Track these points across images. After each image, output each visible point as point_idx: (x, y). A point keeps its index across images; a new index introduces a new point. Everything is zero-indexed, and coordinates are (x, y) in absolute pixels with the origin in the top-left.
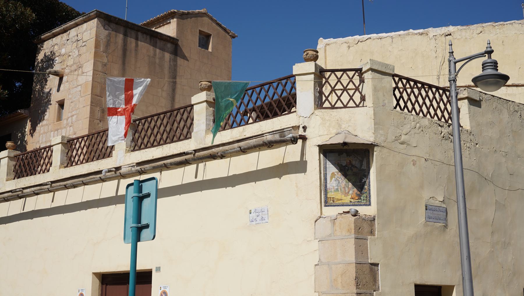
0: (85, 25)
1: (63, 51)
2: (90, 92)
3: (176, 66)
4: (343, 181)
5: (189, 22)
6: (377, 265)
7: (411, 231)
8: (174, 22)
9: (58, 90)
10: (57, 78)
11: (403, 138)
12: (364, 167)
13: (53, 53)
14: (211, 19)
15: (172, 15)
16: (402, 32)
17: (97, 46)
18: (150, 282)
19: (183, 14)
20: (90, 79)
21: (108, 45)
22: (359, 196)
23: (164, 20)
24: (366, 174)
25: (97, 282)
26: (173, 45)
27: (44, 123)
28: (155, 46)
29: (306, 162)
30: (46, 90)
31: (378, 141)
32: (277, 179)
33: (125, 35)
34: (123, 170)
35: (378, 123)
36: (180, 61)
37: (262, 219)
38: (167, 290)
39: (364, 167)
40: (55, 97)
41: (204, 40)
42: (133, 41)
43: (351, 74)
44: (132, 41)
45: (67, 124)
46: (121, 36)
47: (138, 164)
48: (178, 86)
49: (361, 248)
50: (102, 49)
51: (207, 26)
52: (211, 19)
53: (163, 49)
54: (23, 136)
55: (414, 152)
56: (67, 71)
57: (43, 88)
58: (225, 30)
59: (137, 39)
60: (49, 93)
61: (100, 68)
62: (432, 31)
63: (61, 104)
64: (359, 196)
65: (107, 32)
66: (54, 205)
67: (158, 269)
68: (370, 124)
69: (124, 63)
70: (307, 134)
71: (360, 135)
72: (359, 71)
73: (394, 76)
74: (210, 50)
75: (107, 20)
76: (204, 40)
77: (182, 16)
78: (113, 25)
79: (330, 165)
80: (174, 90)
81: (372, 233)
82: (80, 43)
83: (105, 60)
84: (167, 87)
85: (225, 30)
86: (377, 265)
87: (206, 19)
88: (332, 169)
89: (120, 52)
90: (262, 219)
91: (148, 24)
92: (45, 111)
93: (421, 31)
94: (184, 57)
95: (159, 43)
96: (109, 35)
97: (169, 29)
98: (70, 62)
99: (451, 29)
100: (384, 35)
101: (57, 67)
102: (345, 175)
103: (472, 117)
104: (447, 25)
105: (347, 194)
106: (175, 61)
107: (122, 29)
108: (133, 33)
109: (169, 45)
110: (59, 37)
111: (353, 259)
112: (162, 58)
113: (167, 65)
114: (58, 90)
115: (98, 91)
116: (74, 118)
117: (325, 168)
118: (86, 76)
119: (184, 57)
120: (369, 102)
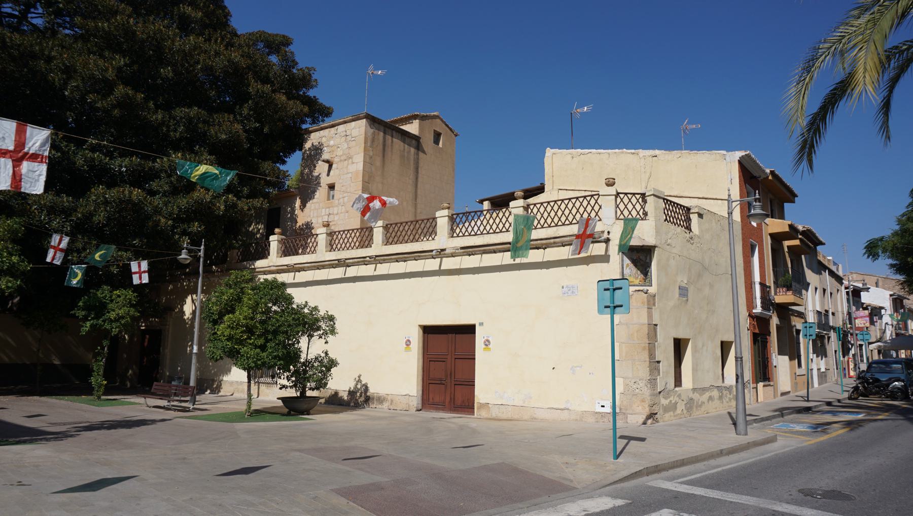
0: (353, 123)
1: (332, 143)
2: (361, 179)
3: (418, 159)
4: (634, 270)
5: (427, 122)
6: (656, 325)
7: (671, 304)
8: (416, 123)
9: (328, 175)
10: (327, 165)
11: (669, 241)
12: (648, 261)
13: (321, 144)
14: (442, 120)
15: (415, 117)
16: (617, 150)
17: (365, 143)
18: (474, 333)
19: (423, 116)
20: (361, 168)
21: (373, 141)
22: (645, 280)
23: (408, 120)
24: (649, 265)
25: (421, 332)
26: (414, 141)
27: (314, 201)
28: (404, 142)
29: (609, 256)
30: (315, 174)
31: (657, 244)
32: (585, 266)
33: (385, 133)
34: (447, 252)
35: (658, 232)
36: (421, 154)
37: (573, 292)
38: (490, 339)
39: (648, 261)
40: (325, 181)
41: (437, 136)
42: (390, 137)
43: (638, 196)
44: (389, 138)
45: (339, 204)
46: (382, 134)
47: (462, 248)
48: (420, 175)
49: (650, 316)
50: (370, 143)
51: (440, 127)
52: (442, 120)
53: (409, 145)
54: (293, 210)
55: (674, 251)
56: (336, 160)
57: (311, 172)
58: (451, 130)
59: (392, 136)
60: (318, 177)
61: (368, 160)
62: (642, 153)
63: (332, 187)
64: (645, 280)
65: (372, 130)
66: (376, 273)
67: (481, 324)
68: (652, 232)
69: (384, 156)
70: (610, 236)
71: (646, 239)
72: (643, 195)
73: (664, 199)
74: (441, 145)
75: (373, 121)
76: (437, 136)
77: (423, 118)
78: (376, 125)
79: (625, 258)
80: (417, 178)
81: (654, 305)
82: (349, 138)
83: (371, 154)
84: (412, 176)
85: (451, 130)
86: (656, 325)
87: (438, 120)
88: (627, 261)
89: (381, 147)
90: (573, 292)
91: (396, 121)
92: (315, 191)
93: (633, 151)
94: (424, 152)
95: (408, 140)
96: (374, 133)
97: (413, 128)
98: (339, 152)
99: (657, 152)
100: (602, 151)
101: (325, 156)
102: (636, 266)
103: (700, 224)
104: (653, 149)
105: (637, 278)
106: (418, 154)
107: (382, 128)
108: (390, 131)
109: (414, 142)
110: (327, 130)
111: (646, 322)
112: (409, 152)
113: (412, 158)
114: (328, 175)
115: (366, 179)
116: (346, 199)
117: (623, 261)
118: (358, 164)
119: (424, 152)
120: (651, 216)
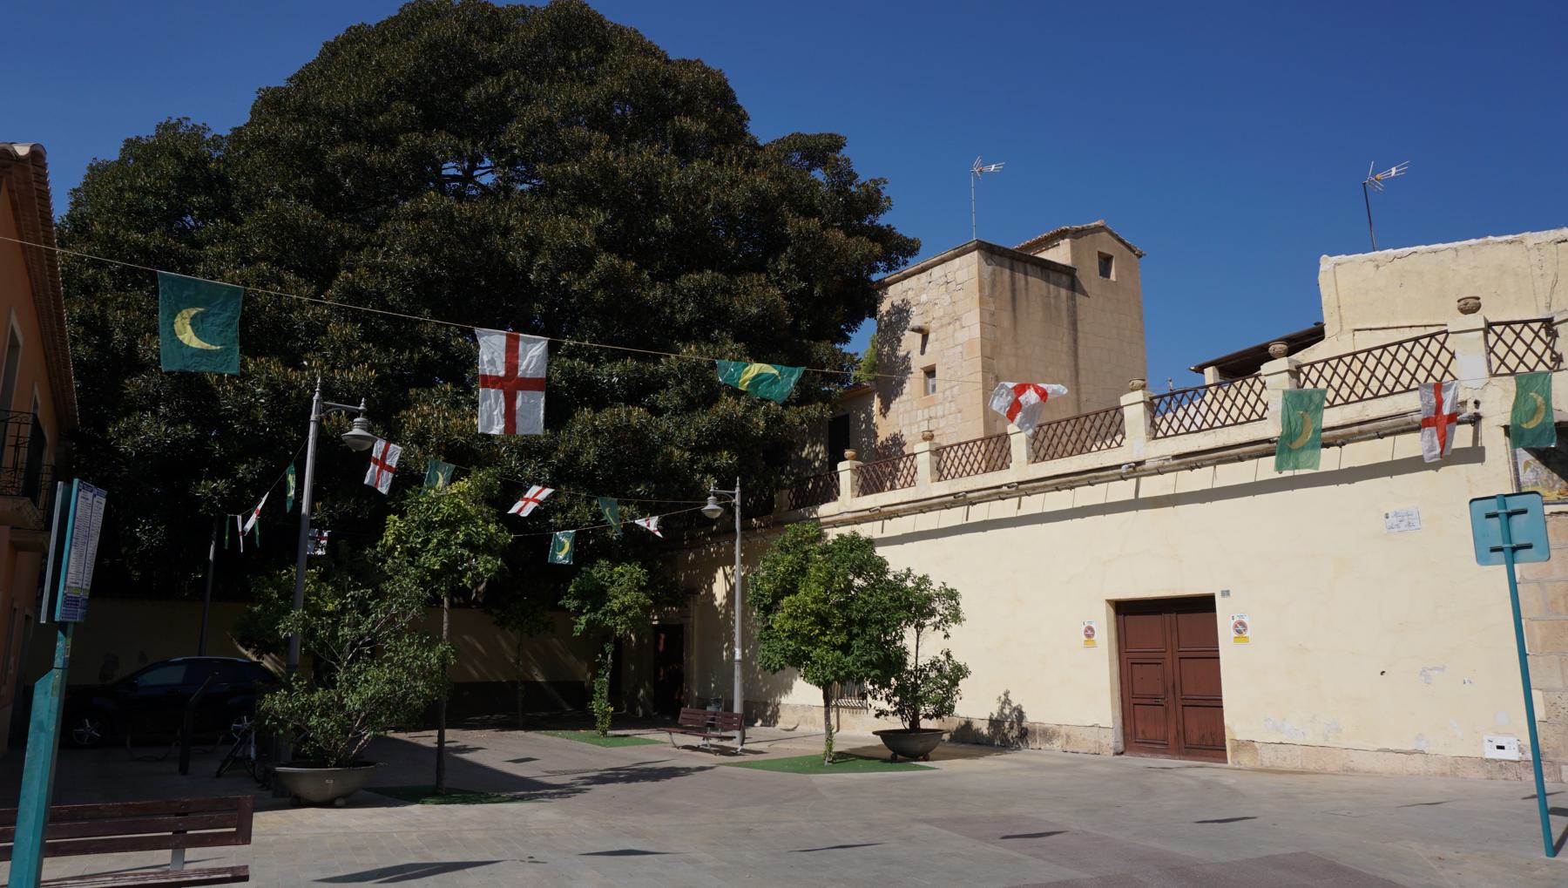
1: (924, 298)
2: (979, 353)
3: (1074, 306)
4: (1544, 472)
9: (923, 352)
10: (919, 336)
13: (906, 302)
14: (1111, 233)
15: (1062, 234)
16: (1473, 241)
19: (1077, 231)
21: (993, 285)
23: (1050, 241)
26: (1066, 276)
27: (903, 398)
28: (1047, 280)
29: (1483, 448)
30: (901, 353)
33: (1012, 269)
36: (1079, 298)
38: (1246, 620)
40: (918, 363)
41: (1105, 262)
43: (1536, 326)
44: (1020, 276)
46: (1007, 272)
47: (1176, 457)
48: (1080, 334)
50: (988, 291)
51: (1107, 245)
52: (1111, 233)
53: (1057, 284)
54: (870, 417)
56: (933, 325)
57: (894, 350)
58: (1129, 247)
59: (1026, 274)
60: (906, 358)
61: (988, 319)
62: (1530, 238)
63: (930, 372)
66: (1021, 513)
67: (1226, 593)
69: (1014, 309)
70: (1480, 410)
72: (1548, 323)
74: (1113, 277)
75: (990, 252)
76: (1105, 262)
77: (1076, 234)
78: (997, 258)
79: (1521, 452)
80: (1075, 341)
82: (952, 286)
84: (1067, 338)
85: (1129, 247)
87: (1105, 234)
88: (1524, 456)
89: (1008, 294)
91: (1030, 247)
92: (902, 383)
93: (1510, 237)
94: (1084, 293)
95: (1053, 276)
96: (993, 273)
97: (1060, 254)
98: (938, 312)
101: (915, 321)
105: (1552, 489)
106: (1073, 299)
107: (1007, 262)
109: (1064, 278)
110: (914, 278)
112: (1058, 296)
113: (1064, 306)
114: (923, 352)
119: (1084, 293)
